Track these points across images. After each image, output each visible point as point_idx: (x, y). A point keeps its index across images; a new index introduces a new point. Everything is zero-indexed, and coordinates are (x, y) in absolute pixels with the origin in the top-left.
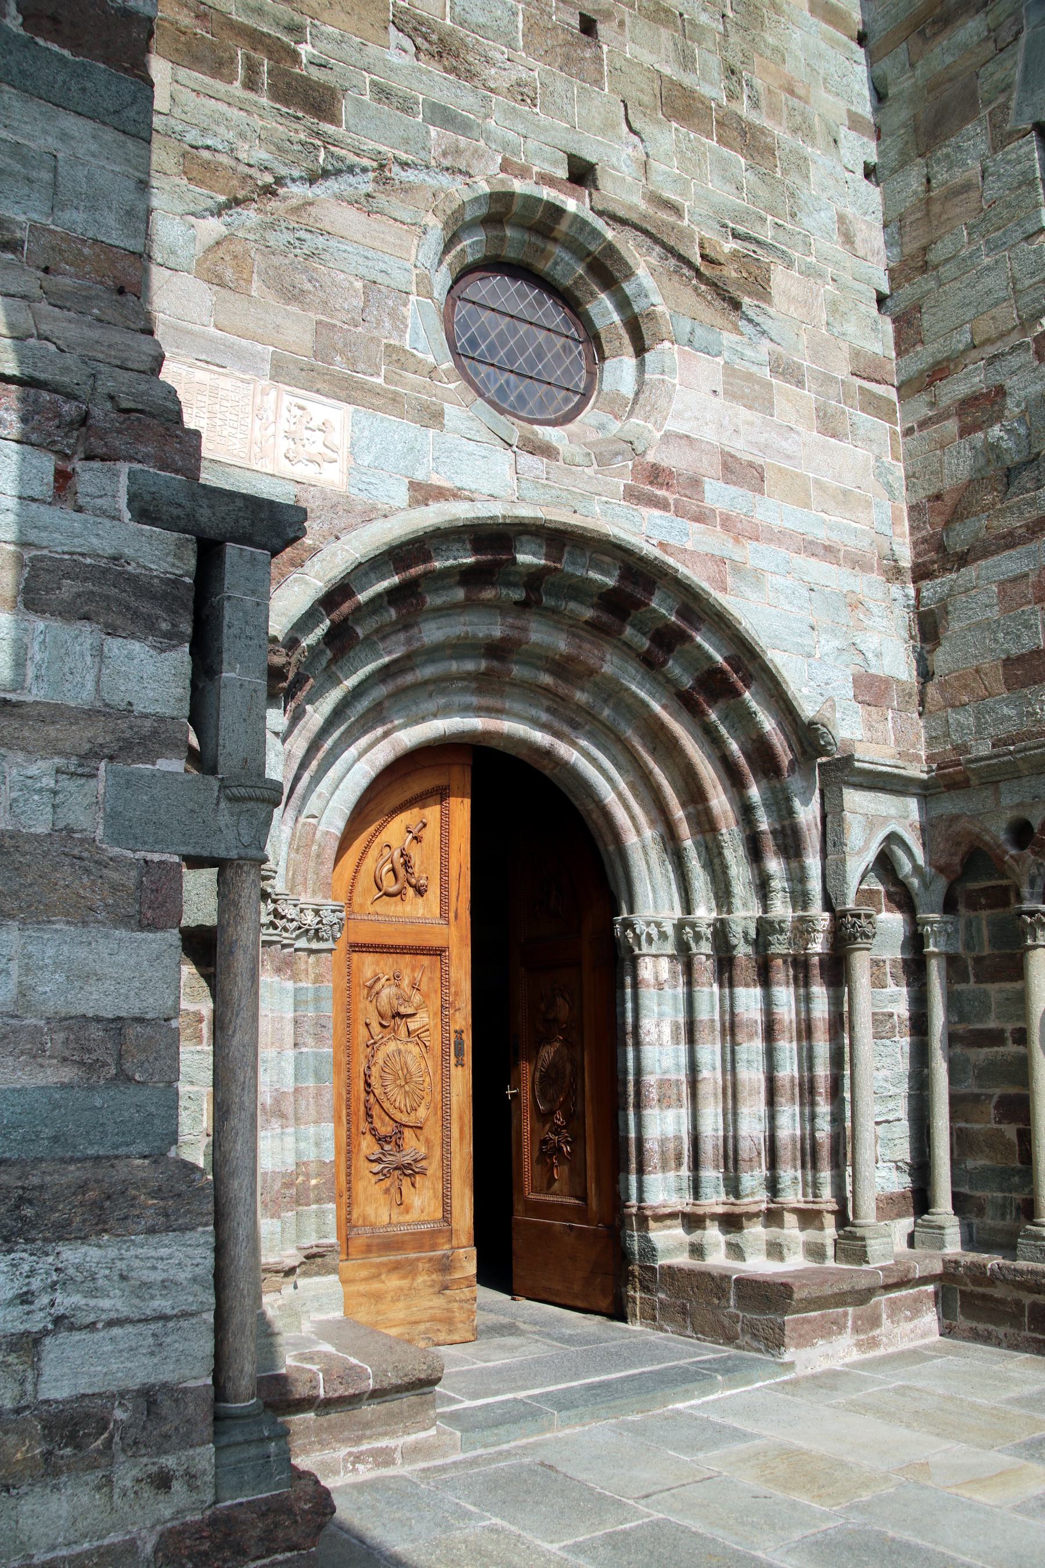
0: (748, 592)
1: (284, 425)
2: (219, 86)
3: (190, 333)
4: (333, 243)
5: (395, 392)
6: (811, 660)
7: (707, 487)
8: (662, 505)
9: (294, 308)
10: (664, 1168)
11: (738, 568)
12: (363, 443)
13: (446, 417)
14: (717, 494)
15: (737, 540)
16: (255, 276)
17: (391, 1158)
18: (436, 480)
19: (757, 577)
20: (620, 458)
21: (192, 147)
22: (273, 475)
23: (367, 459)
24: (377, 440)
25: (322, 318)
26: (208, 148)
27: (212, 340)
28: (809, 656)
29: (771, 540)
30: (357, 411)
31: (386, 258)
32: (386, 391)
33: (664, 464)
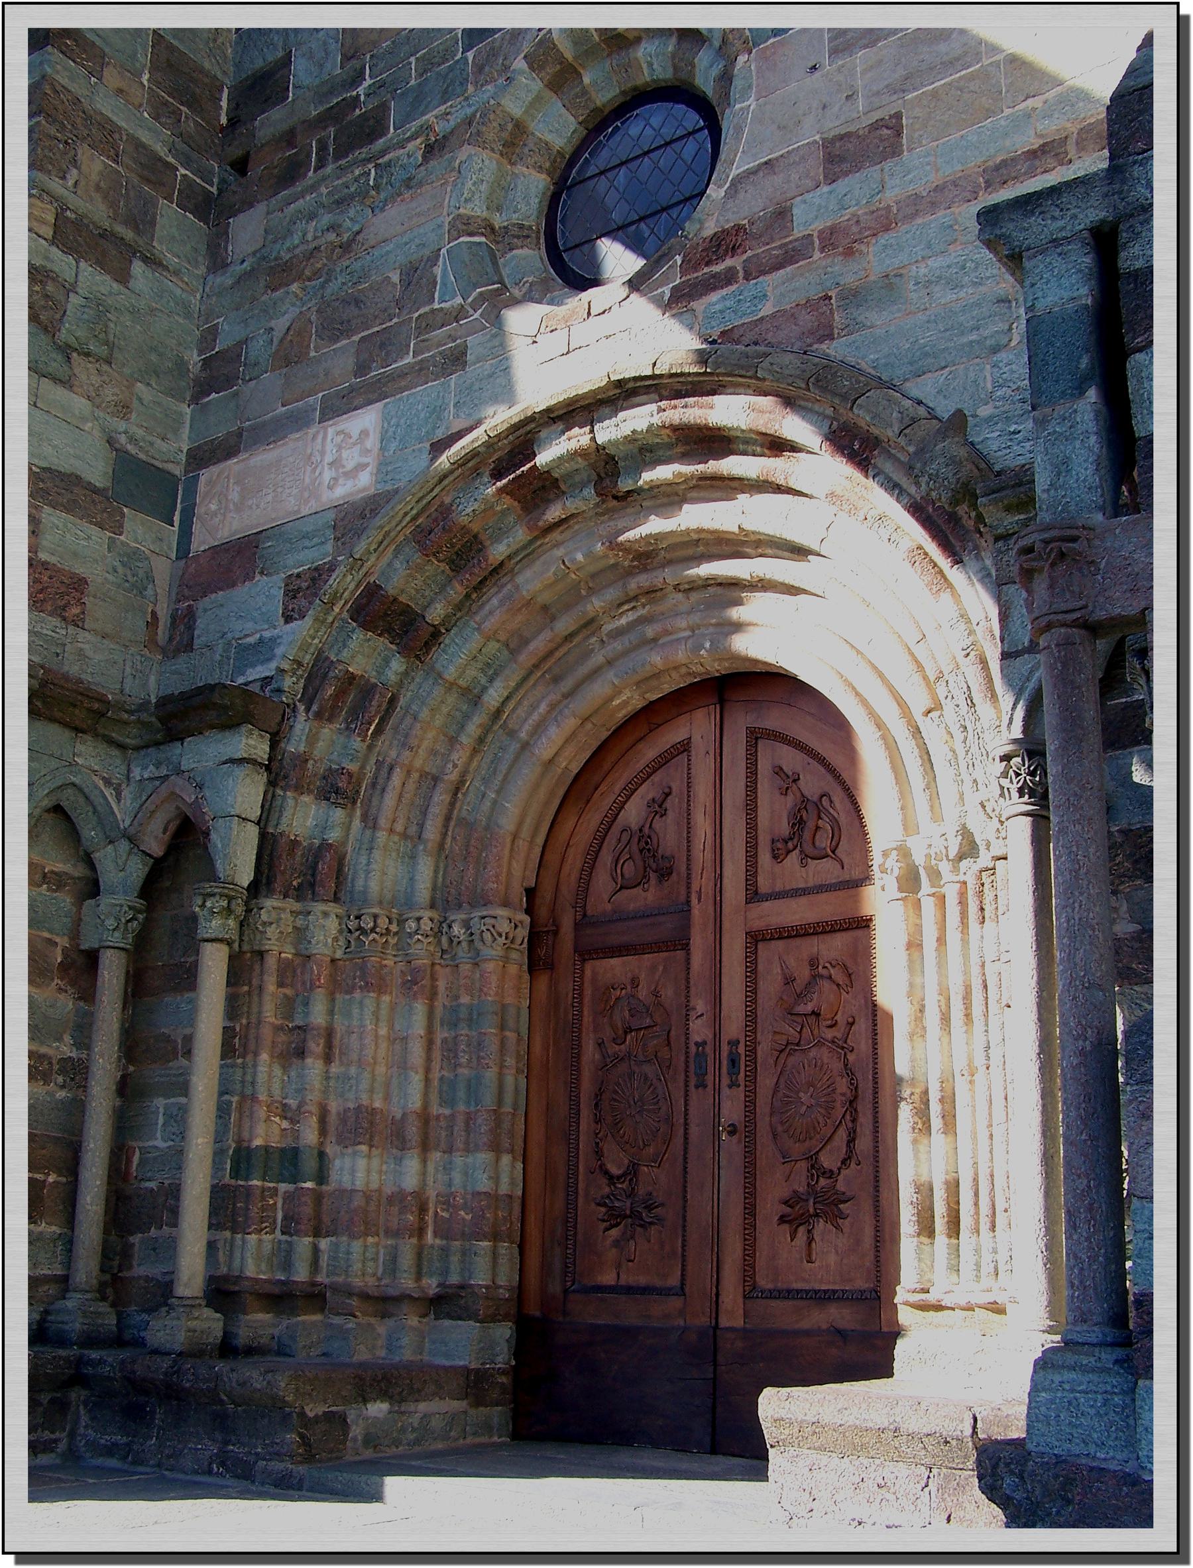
1: (329, 458)
2: (299, 187)
3: (264, 424)
4: (376, 253)
6: (1003, 356)
7: (795, 211)
8: (728, 278)
11: (853, 296)
12: (390, 433)
19: (890, 283)
21: (276, 259)
23: (393, 446)
25: (363, 334)
27: (277, 420)
28: (995, 350)
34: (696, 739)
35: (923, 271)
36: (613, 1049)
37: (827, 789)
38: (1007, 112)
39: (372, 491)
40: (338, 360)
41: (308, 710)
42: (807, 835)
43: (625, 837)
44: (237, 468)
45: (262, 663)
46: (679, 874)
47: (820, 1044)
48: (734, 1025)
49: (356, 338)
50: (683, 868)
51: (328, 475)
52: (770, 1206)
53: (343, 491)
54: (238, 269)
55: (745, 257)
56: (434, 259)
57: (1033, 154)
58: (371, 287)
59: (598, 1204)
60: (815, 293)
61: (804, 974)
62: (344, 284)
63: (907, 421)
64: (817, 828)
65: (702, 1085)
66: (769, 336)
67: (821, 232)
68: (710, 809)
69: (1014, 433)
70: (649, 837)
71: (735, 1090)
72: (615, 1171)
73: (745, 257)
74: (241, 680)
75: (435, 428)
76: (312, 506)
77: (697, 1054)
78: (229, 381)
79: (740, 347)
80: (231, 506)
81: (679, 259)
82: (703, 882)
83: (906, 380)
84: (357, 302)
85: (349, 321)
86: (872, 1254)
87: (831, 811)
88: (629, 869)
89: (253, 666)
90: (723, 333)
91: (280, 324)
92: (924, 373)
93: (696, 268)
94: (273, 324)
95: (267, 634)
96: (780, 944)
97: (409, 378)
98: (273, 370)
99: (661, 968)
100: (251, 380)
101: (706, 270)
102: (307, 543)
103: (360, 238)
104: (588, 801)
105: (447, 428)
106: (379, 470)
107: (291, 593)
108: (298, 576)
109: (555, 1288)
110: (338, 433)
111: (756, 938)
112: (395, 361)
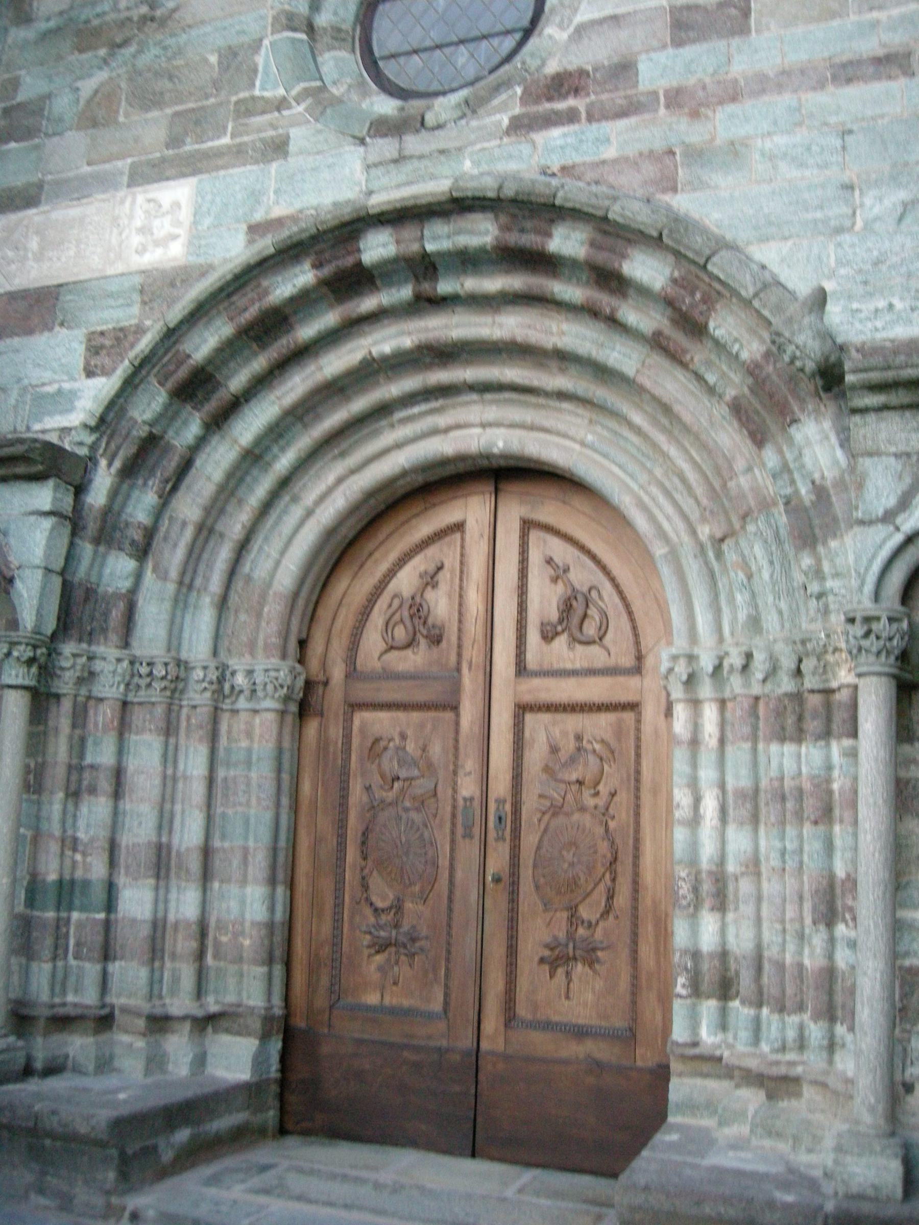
0: (718, 179)
1: (138, 223)
3: (66, 181)
4: (194, 33)
5: (240, 144)
6: (846, 238)
7: (642, 67)
8: (571, 117)
9: (155, 114)
10: (696, 991)
11: (697, 155)
12: (204, 209)
13: (292, 143)
14: (657, 70)
15: (695, 114)
16: (123, 103)
17: (382, 934)
18: (277, 212)
19: (735, 152)
20: (502, 90)
22: (122, 275)
23: (207, 222)
24: (218, 199)
26: (98, 15)
28: (839, 230)
29: (763, 91)
30: (200, 181)
31: (243, 18)
32: (229, 147)
33: (570, 68)
34: (471, 524)
35: (768, 145)
36: (379, 794)
37: (595, 583)
38: (853, 18)
39: (182, 262)
40: (150, 130)
41: (110, 465)
42: (575, 620)
43: (396, 603)
44: (37, 219)
45: (62, 412)
46: (449, 641)
47: (583, 809)
48: (500, 785)
49: (169, 111)
50: (454, 639)
51: (136, 240)
52: (532, 945)
53: (153, 258)
54: (43, 26)
55: (588, 100)
56: (256, 45)
57: (878, 61)
58: (187, 65)
59: (366, 933)
60: (659, 145)
61: (569, 746)
62: (156, 56)
63: (759, 285)
64: (585, 616)
65: (468, 835)
66: (611, 179)
67: (666, 92)
68: (483, 588)
69: (858, 311)
70: (421, 605)
71: (500, 844)
72: (380, 904)
73: (588, 100)
74: (37, 427)
75: (252, 210)
76: (120, 268)
77: (465, 807)
78: (29, 133)
79: (581, 184)
80: (30, 255)
81: (519, 90)
82: (473, 653)
83: (749, 243)
84: (171, 78)
85: (162, 94)
86: (628, 998)
87: (600, 603)
88: (400, 634)
89: (50, 414)
90: (564, 169)
91: (88, 86)
92: (768, 240)
93: (537, 100)
94: (79, 84)
95: (66, 386)
96: (546, 717)
97: (226, 158)
98: (79, 128)
99: (429, 726)
100: (54, 134)
101: (548, 106)
102: (111, 302)
103: (176, 16)
104: (361, 566)
105: (267, 213)
106: (190, 243)
107: (94, 349)
108: (102, 333)
109: (321, 1002)
110: (149, 201)
111: (522, 709)
112: (212, 140)
